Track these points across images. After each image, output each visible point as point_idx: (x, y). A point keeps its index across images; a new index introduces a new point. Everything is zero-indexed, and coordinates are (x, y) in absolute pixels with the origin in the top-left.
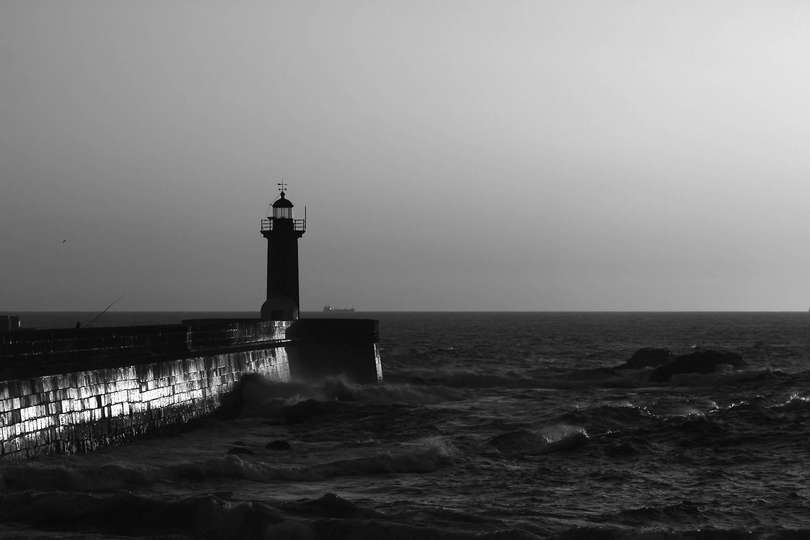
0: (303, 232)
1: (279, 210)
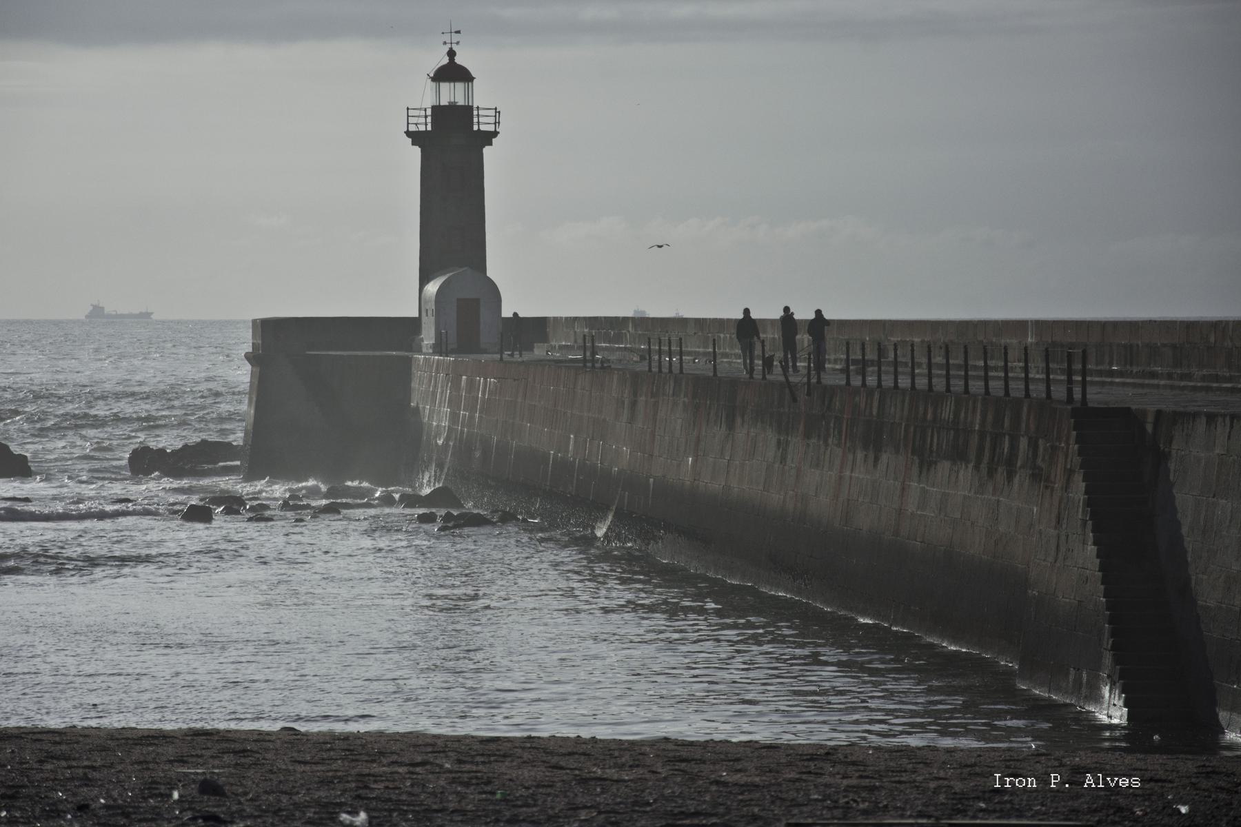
0: (495, 134)
1: (445, 86)
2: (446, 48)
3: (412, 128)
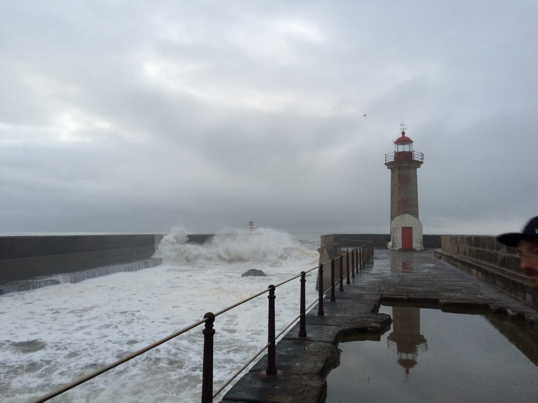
0: (422, 163)
2: (402, 131)
3: (387, 162)
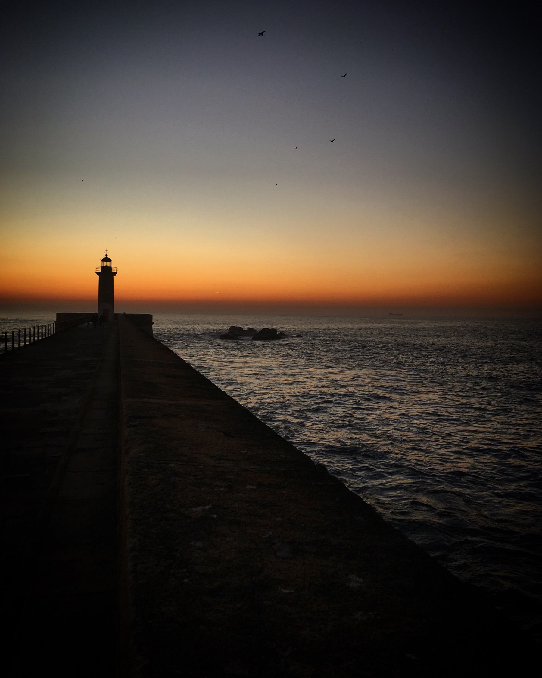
0: (116, 273)
1: (105, 263)
